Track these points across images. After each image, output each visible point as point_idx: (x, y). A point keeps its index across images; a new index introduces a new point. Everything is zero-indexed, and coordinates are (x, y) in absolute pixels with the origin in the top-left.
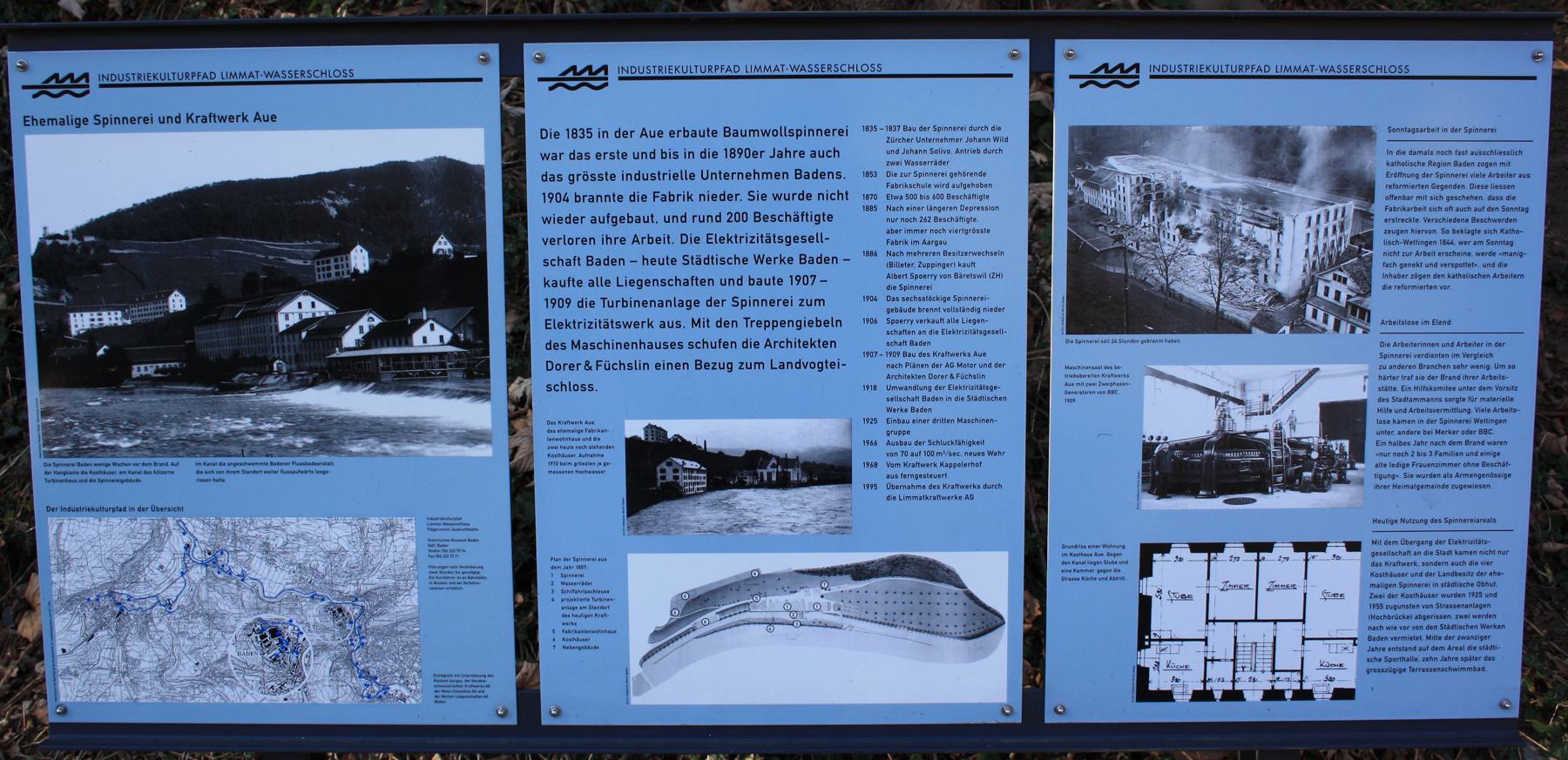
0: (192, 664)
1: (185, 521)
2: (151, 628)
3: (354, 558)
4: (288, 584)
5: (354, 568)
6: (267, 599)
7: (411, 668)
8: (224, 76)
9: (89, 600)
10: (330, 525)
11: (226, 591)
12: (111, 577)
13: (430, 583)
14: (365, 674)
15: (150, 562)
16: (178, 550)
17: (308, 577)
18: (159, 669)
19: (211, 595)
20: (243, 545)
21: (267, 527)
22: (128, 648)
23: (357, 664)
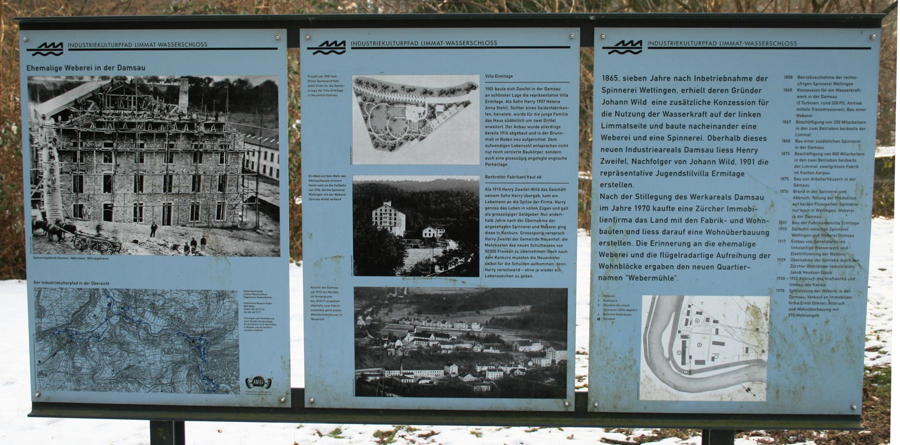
0: (110, 370)
3: (201, 312)
5: (201, 318)
7: (232, 375)
10: (189, 294)
14: (208, 378)
15: (89, 313)
18: (92, 373)
23: (202, 372)
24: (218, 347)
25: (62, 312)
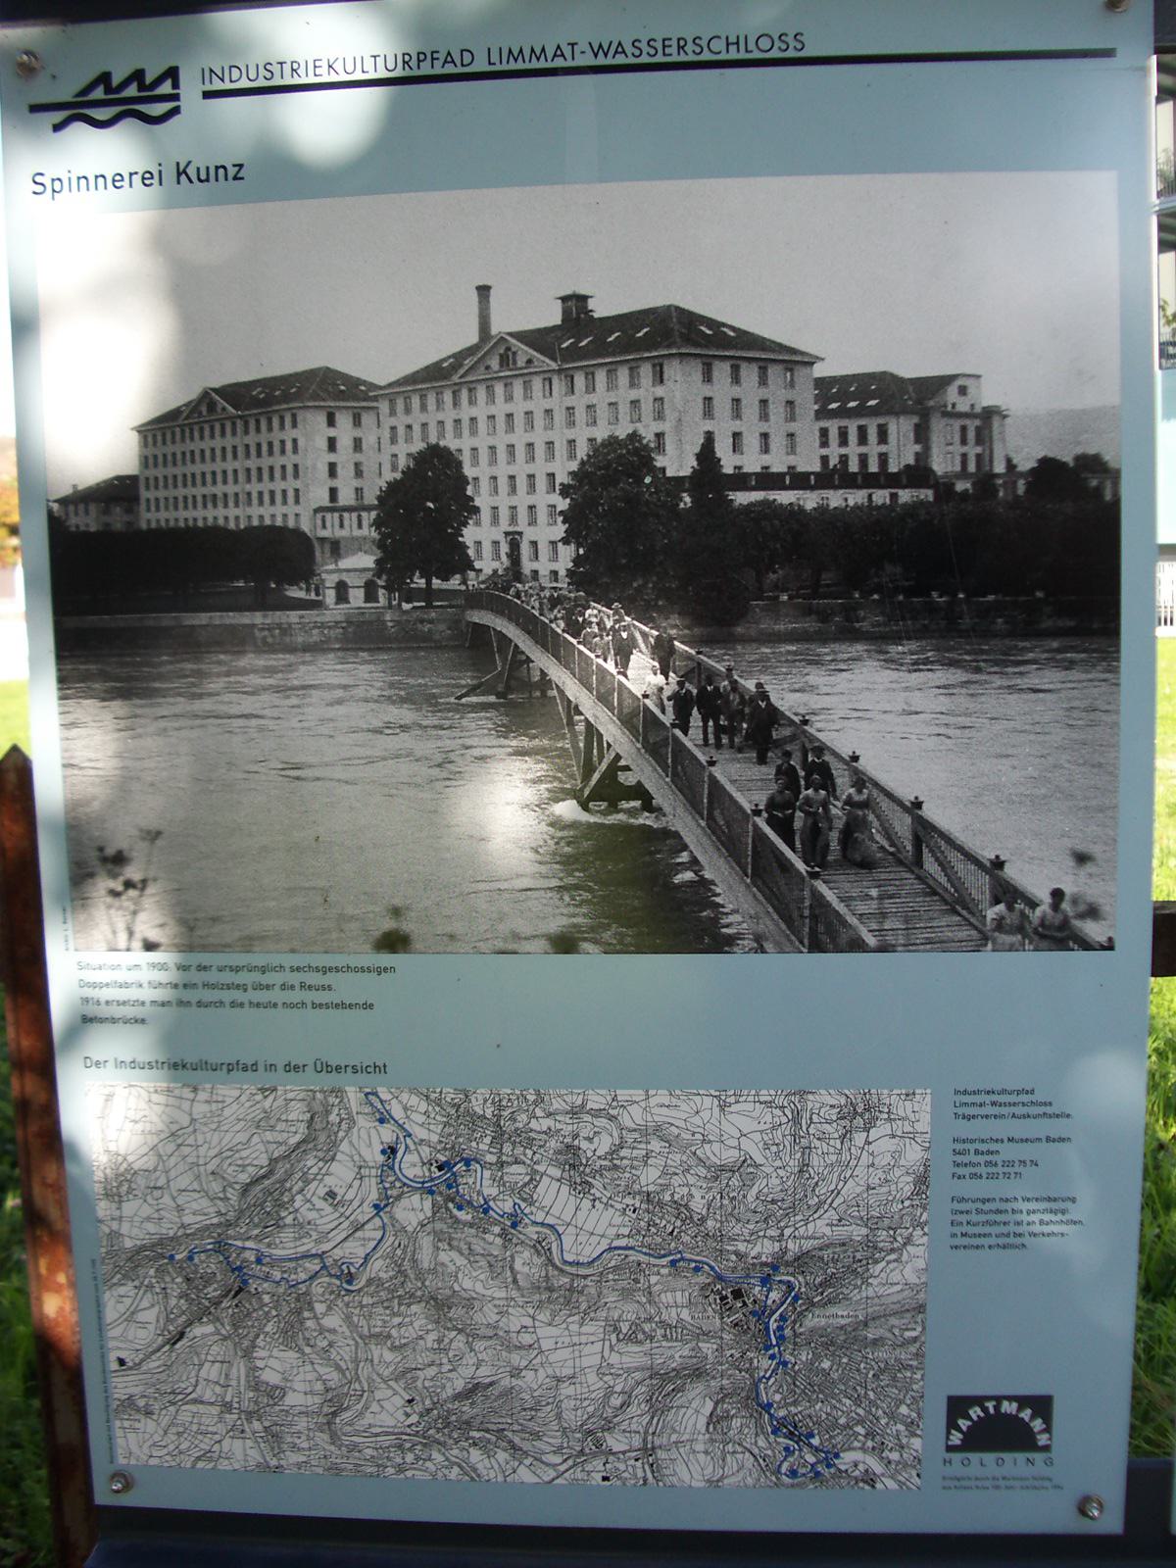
0: (399, 1401)
1: (385, 1096)
2: (309, 1324)
3: (775, 1181)
4: (618, 1236)
5: (773, 1202)
6: (568, 1268)
7: (892, 1416)
8: (495, 58)
9: (172, 1257)
10: (722, 1108)
11: (478, 1249)
12: (219, 1213)
13: (954, 1235)
15: (307, 1182)
16: (368, 1158)
17: (667, 1222)
18: (326, 1410)
19: (443, 1257)
20: (519, 1150)
21: (575, 1112)
22: (260, 1364)
23: (770, 1405)
24: (840, 1315)
25: (198, 1177)
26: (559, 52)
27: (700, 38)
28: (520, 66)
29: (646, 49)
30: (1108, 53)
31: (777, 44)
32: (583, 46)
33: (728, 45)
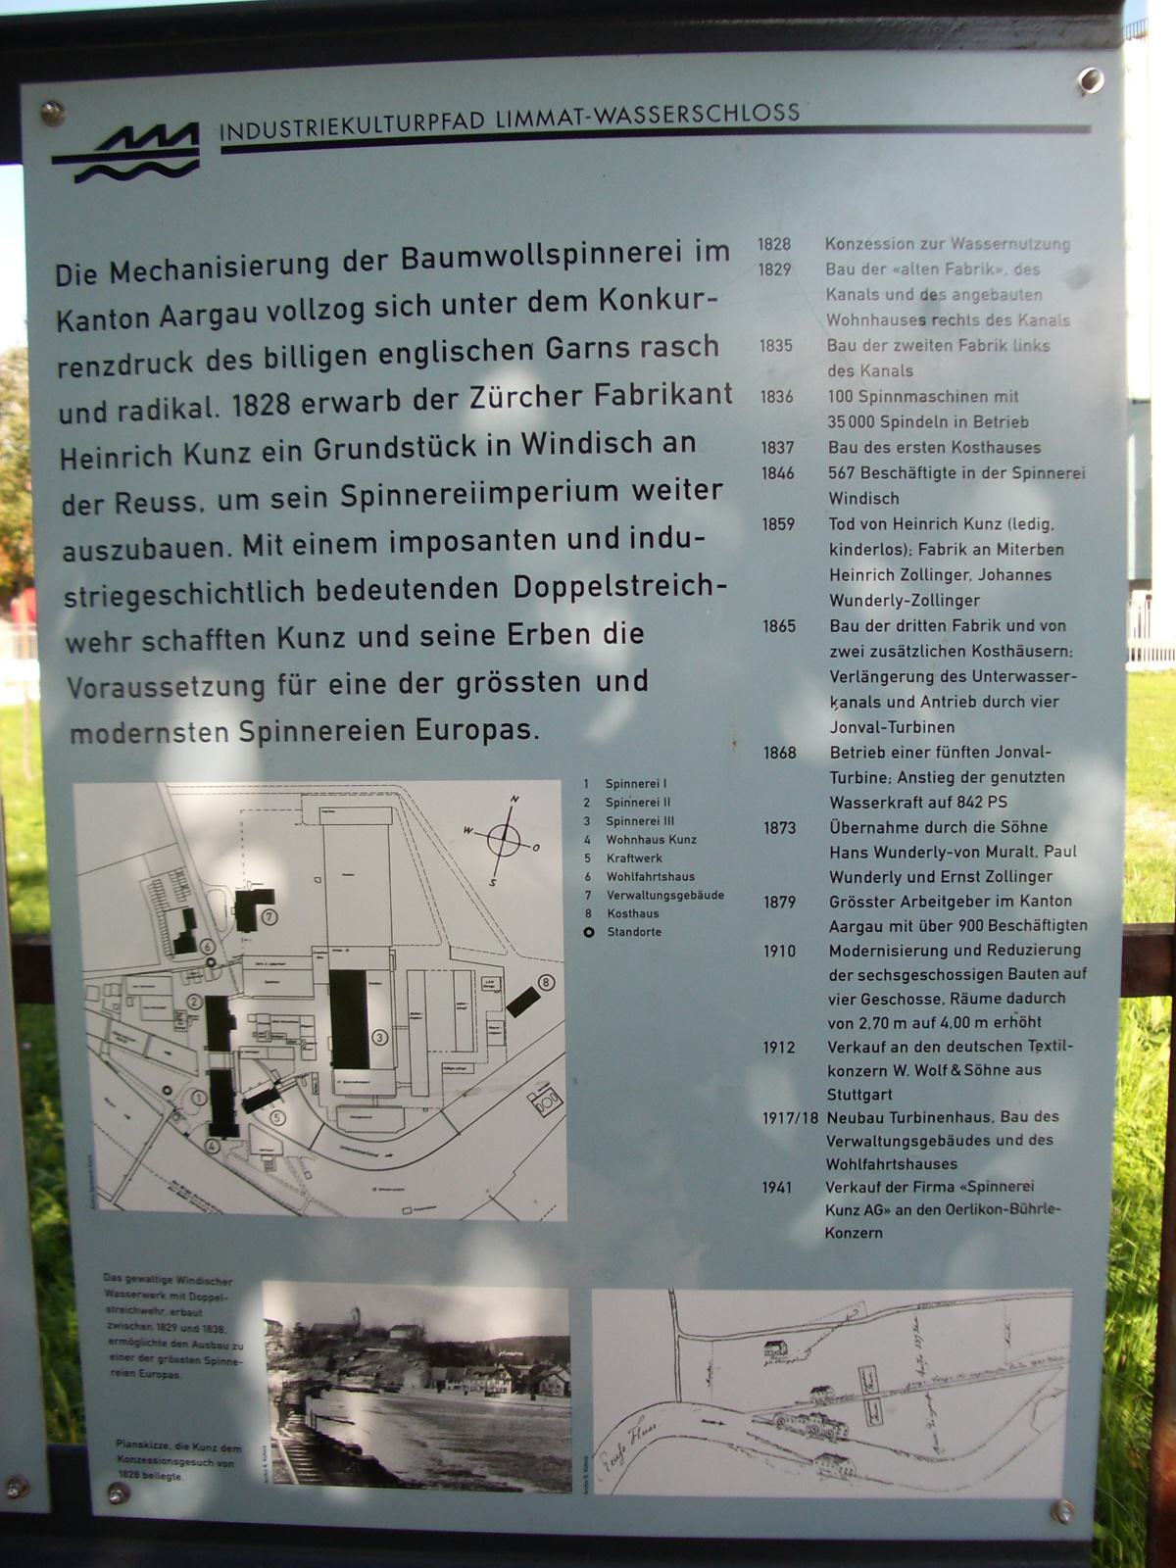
8: (504, 121)
26: (565, 117)
27: (700, 107)
28: (528, 128)
29: (648, 115)
30: (1084, 130)
31: (773, 113)
32: (588, 111)
33: (726, 113)
